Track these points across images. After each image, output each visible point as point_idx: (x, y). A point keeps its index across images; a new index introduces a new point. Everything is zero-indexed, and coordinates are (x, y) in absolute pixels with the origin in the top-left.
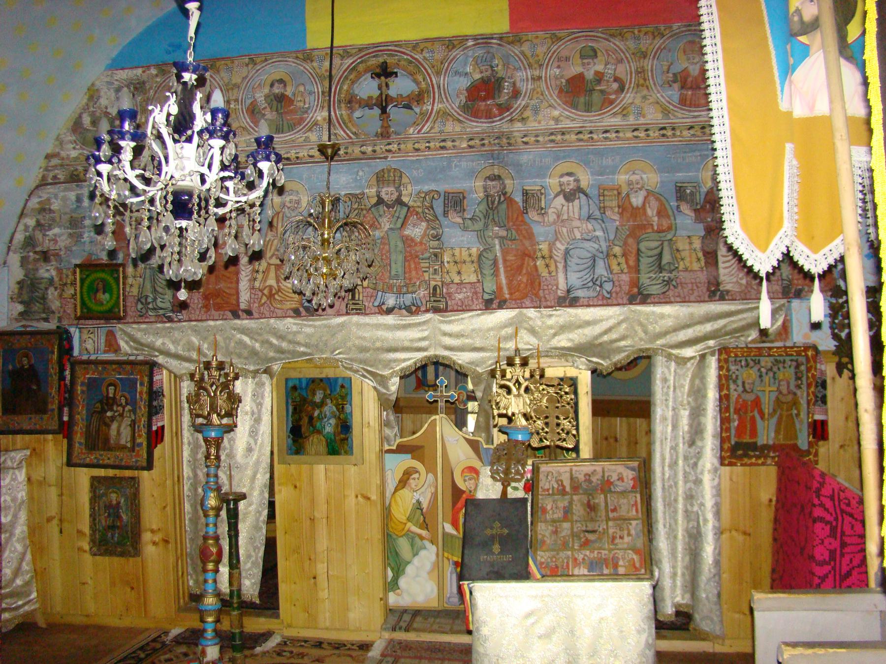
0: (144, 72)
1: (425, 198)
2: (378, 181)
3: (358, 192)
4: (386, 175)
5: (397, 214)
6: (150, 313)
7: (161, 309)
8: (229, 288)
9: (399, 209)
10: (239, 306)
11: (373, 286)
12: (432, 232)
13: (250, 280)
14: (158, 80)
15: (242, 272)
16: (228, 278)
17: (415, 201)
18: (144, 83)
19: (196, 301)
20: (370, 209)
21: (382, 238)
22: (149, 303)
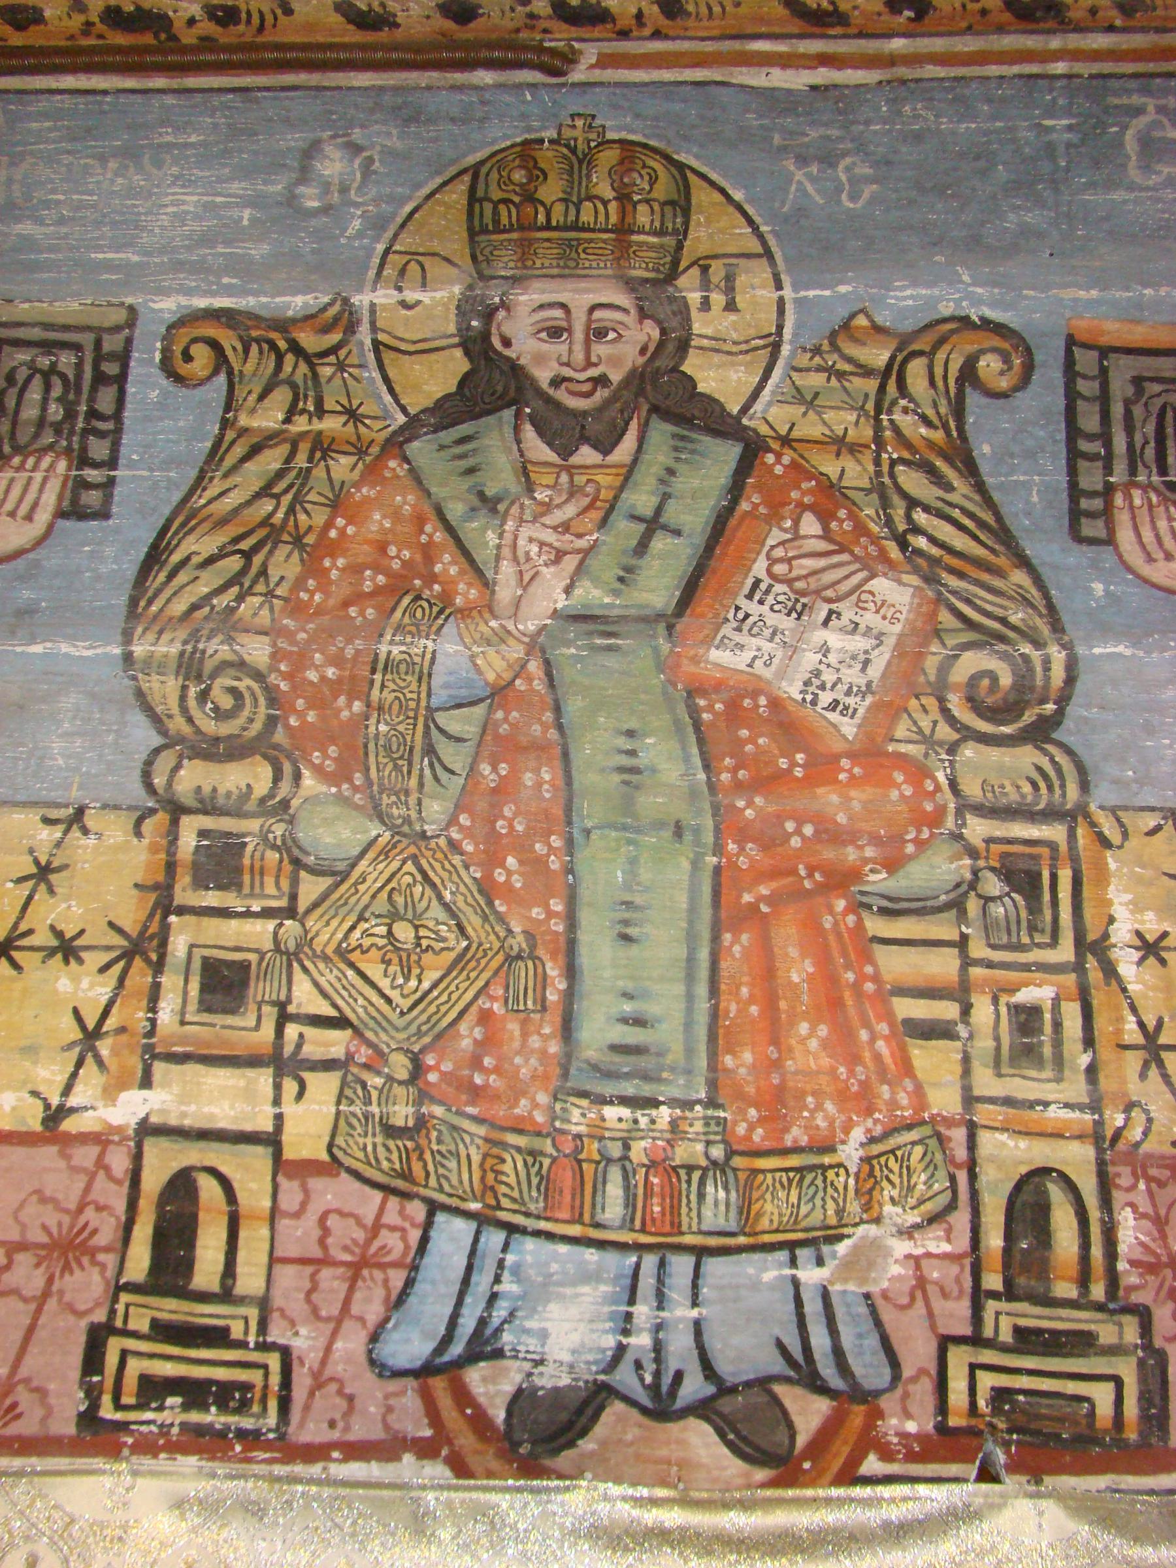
1: (894, 372)
2: (472, 234)
3: (297, 303)
4: (550, 191)
5: (642, 499)
9: (659, 454)
11: (389, 1157)
12: (972, 662)
17: (809, 401)
20: (396, 443)
21: (499, 694)
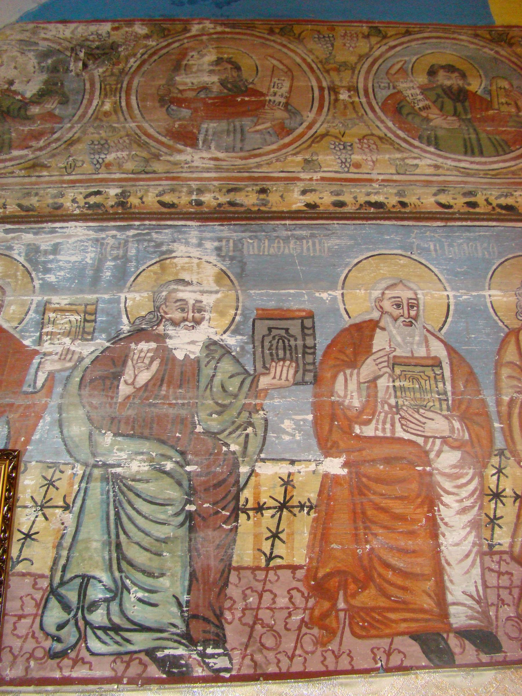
0: (115, 29)
6: (95, 645)
7: (143, 628)
8: (404, 552)
10: (445, 615)
13: (475, 525)
14: (152, 43)
15: (446, 499)
16: (402, 518)
18: (114, 47)
19: (282, 601)
22: (94, 606)
